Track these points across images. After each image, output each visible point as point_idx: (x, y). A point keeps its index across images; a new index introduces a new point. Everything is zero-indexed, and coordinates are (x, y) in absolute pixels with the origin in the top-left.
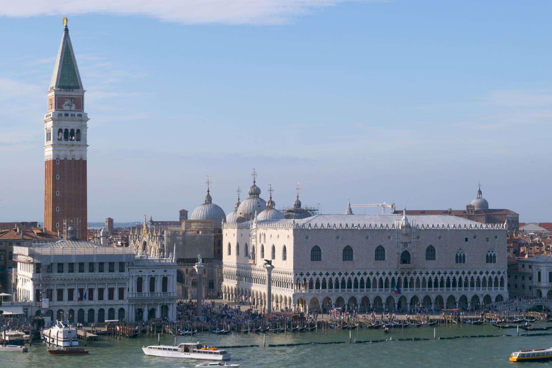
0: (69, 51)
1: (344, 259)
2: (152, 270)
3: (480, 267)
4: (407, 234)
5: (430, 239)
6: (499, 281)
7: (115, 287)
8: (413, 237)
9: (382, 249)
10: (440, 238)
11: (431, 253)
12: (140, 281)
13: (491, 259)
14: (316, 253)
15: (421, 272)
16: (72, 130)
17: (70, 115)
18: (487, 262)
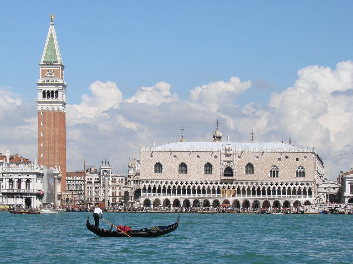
3: (290, 180)
4: (229, 155)
8: (234, 157)
11: (250, 168)
12: (11, 181)
16: (52, 91)
17: (50, 81)
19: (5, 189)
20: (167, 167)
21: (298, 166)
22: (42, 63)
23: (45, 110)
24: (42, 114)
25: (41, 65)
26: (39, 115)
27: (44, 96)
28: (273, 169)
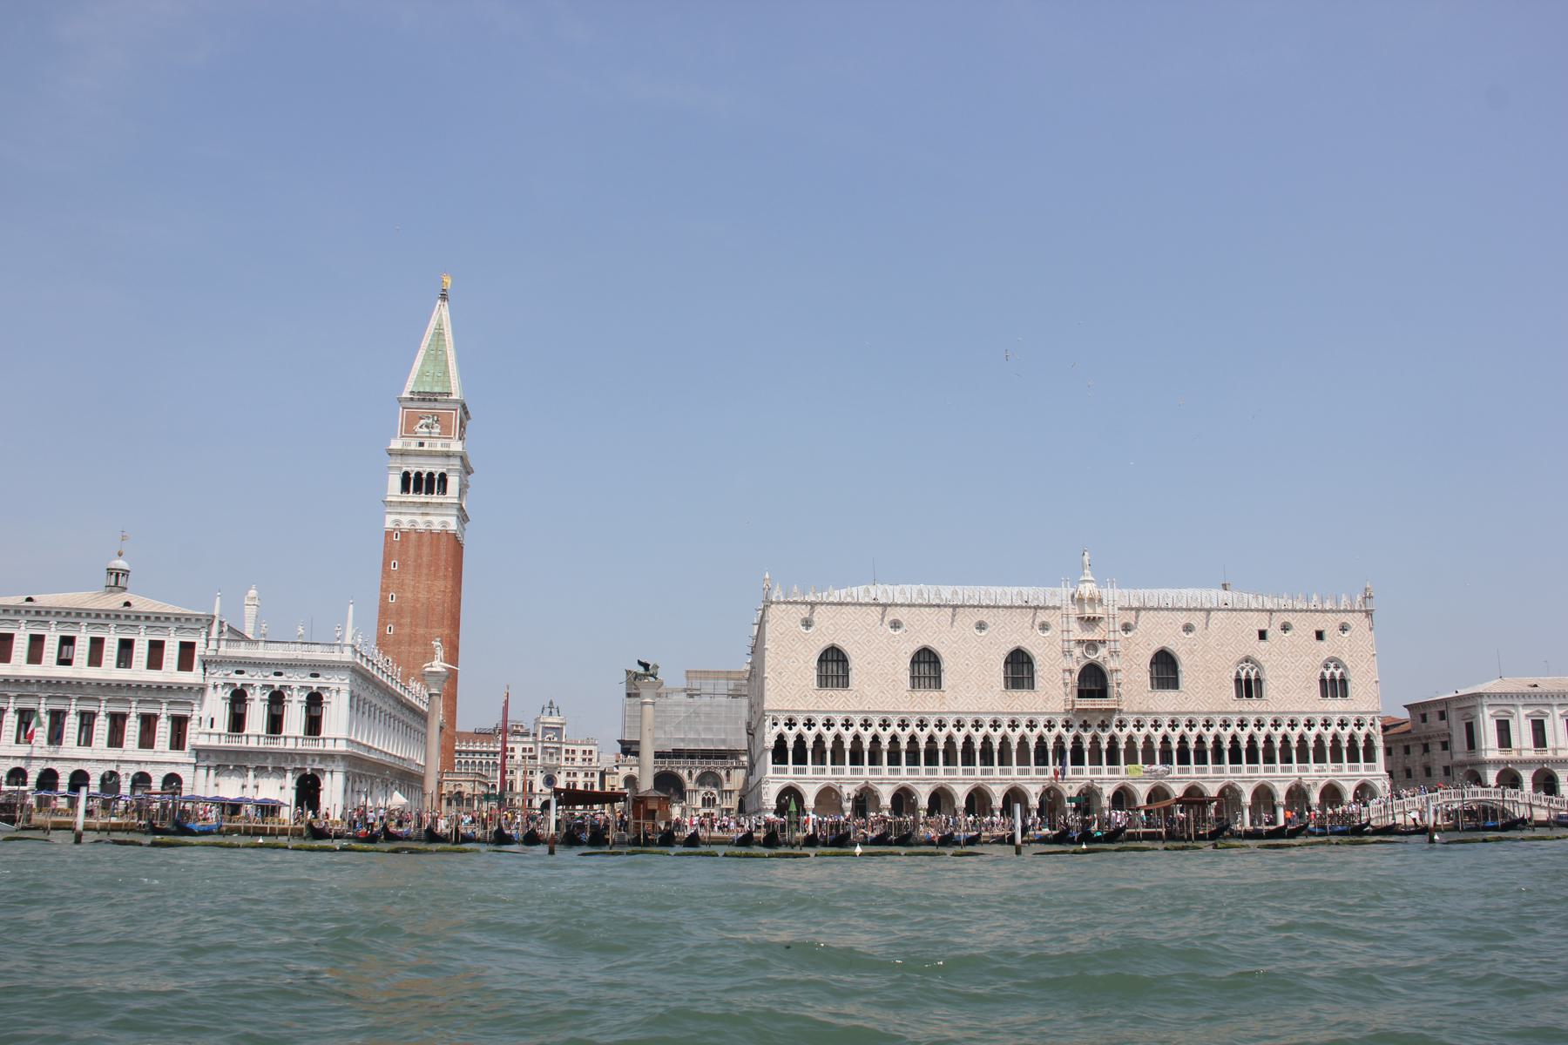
0: (441, 331)
1: (917, 684)
2: (274, 670)
3: (1304, 710)
4: (1094, 618)
5: (1160, 631)
6: (1361, 744)
7: (158, 712)
9: (1025, 660)
10: (1188, 628)
11: (1165, 669)
12: (238, 698)
13: (1334, 686)
14: (835, 668)
15: (1138, 721)
16: (431, 475)
17: (426, 444)
18: (1324, 694)
19: (208, 729)
20: (869, 664)
21: (1326, 657)
22: (406, 395)
23: (405, 526)
24: (396, 537)
25: (400, 400)
26: (386, 540)
27: (405, 488)
28: (1245, 671)
